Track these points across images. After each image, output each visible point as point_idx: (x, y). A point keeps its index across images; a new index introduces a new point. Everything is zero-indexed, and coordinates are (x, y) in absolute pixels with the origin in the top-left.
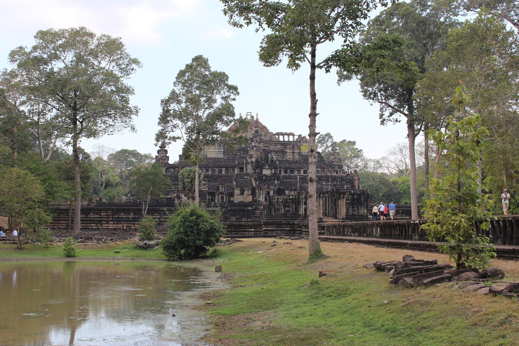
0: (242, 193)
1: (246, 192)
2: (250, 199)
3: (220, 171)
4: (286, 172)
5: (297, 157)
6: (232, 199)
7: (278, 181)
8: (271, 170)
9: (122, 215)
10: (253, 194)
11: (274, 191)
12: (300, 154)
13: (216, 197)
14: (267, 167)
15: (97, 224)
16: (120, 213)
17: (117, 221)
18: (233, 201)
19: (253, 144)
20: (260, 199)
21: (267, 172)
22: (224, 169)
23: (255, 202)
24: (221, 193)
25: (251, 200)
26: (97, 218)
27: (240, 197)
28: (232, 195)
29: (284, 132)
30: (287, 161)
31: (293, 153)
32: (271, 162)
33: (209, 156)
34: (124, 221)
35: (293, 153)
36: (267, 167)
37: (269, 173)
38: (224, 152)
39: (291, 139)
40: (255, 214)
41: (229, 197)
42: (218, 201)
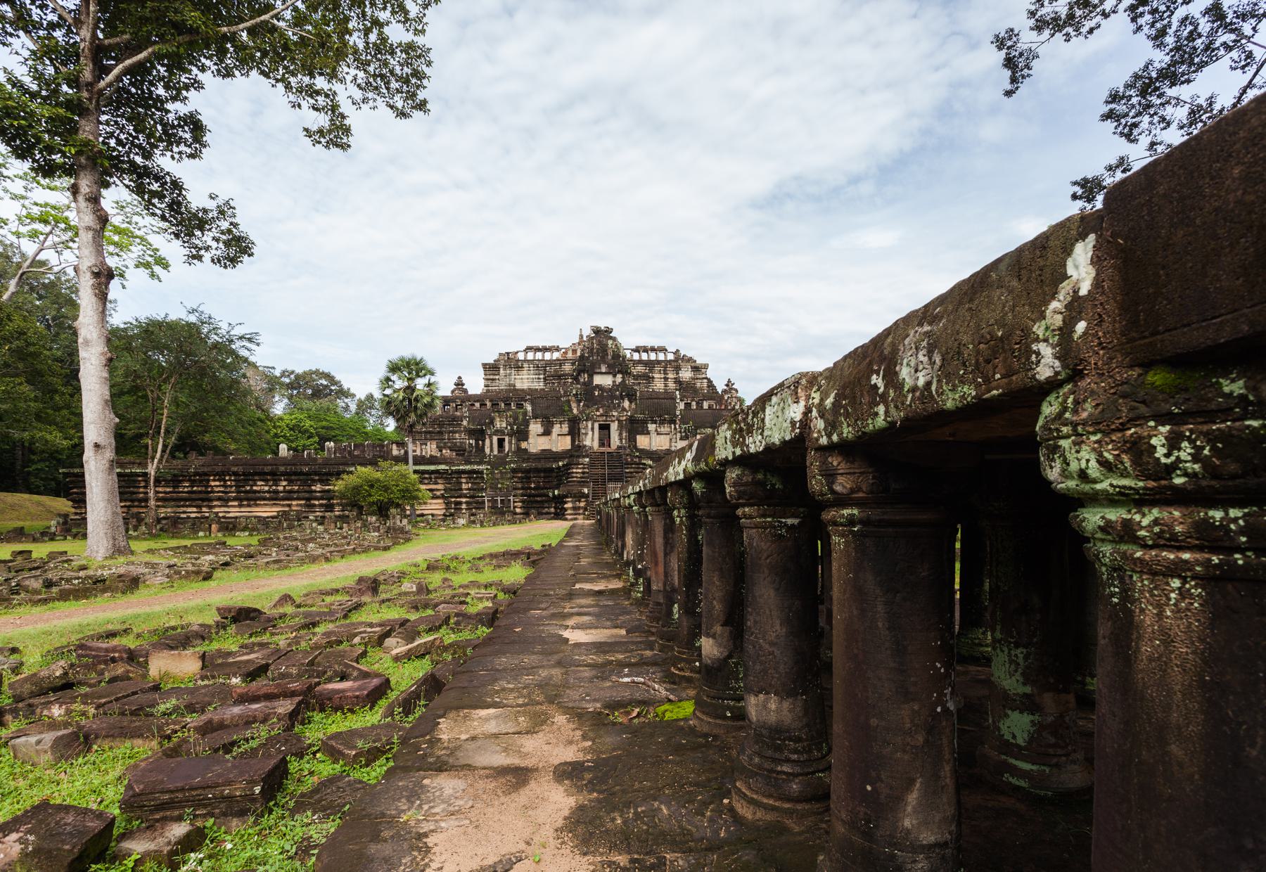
0: (547, 433)
1: (556, 429)
2: (565, 444)
5: (672, 385)
6: (524, 445)
8: (615, 376)
9: (260, 486)
10: (574, 432)
13: (487, 442)
15: (199, 507)
16: (255, 481)
17: (248, 499)
20: (588, 442)
23: (577, 450)
24: (497, 432)
26: (200, 492)
27: (543, 439)
28: (523, 435)
31: (666, 379)
33: (519, 386)
34: (265, 499)
35: (666, 379)
39: (661, 357)
40: (569, 475)
42: (492, 450)
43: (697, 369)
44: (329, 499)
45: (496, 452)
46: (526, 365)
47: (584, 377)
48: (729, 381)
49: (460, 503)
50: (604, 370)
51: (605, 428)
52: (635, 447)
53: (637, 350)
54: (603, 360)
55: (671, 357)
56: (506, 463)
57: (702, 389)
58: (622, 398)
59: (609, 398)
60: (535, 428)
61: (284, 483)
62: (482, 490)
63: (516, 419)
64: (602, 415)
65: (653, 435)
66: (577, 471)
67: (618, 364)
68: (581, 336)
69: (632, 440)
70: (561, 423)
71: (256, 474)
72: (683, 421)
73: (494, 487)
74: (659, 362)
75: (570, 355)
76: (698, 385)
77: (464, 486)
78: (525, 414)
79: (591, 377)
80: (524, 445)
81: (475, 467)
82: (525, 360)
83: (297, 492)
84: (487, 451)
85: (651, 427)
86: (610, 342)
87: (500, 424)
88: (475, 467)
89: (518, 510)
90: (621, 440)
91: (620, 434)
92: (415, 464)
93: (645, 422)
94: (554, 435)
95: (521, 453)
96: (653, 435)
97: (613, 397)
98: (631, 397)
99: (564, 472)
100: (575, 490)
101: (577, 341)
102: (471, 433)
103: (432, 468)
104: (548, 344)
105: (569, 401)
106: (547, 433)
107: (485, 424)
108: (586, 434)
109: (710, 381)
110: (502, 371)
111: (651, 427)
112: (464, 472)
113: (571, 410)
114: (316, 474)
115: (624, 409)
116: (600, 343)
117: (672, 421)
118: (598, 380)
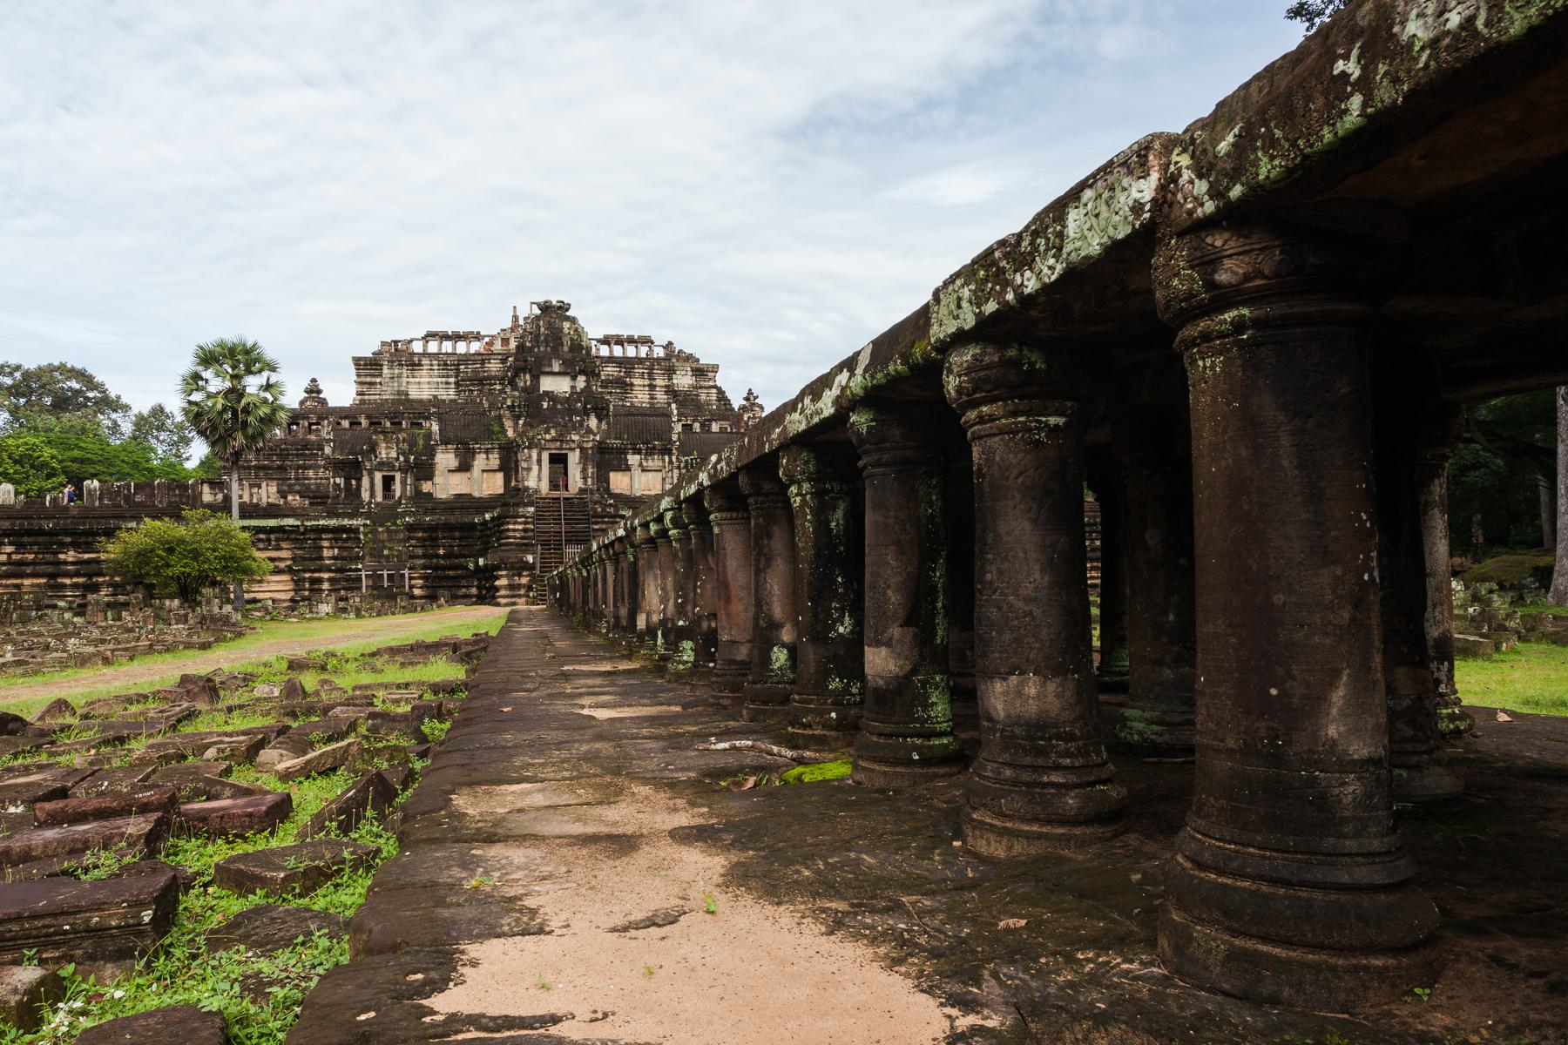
0: (465, 467)
1: (480, 461)
2: (494, 485)
5: (661, 397)
6: (426, 487)
8: (574, 378)
10: (509, 467)
11: (582, 449)
13: (365, 481)
14: (556, 367)
18: (429, 494)
20: (531, 483)
21: (556, 385)
23: (514, 496)
24: (382, 465)
25: (501, 491)
28: (424, 470)
29: (625, 333)
32: (571, 350)
33: (414, 394)
35: (652, 387)
36: (556, 367)
37: (567, 389)
38: (457, 383)
40: (502, 534)
41: (418, 479)
42: (372, 495)
43: (700, 372)
44: (90, 576)
45: (379, 498)
46: (425, 361)
47: (525, 380)
48: (750, 392)
49: (320, 581)
50: (556, 368)
51: (559, 460)
52: (607, 490)
53: (606, 341)
54: (556, 353)
55: (659, 352)
56: (398, 516)
57: (708, 403)
58: (586, 413)
59: (565, 412)
60: (445, 459)
61: (9, 549)
62: (357, 558)
64: (553, 440)
65: (636, 472)
66: (515, 528)
67: (579, 359)
68: (515, 318)
69: (602, 479)
70: (487, 452)
72: (683, 451)
73: (376, 555)
74: (640, 361)
75: (498, 347)
76: (703, 397)
77: (326, 553)
78: (429, 436)
79: (536, 379)
80: (426, 487)
81: (346, 522)
82: (425, 354)
83: (33, 563)
84: (365, 496)
85: (633, 459)
86: (566, 325)
87: (386, 452)
88: (346, 522)
89: (417, 592)
90: (585, 478)
91: (584, 470)
92: (242, 517)
93: (622, 452)
94: (476, 470)
95: (423, 501)
96: (636, 472)
97: (571, 411)
98: (601, 411)
99: (494, 530)
100: (513, 557)
102: (338, 466)
103: (272, 523)
104: (462, 329)
105: (500, 418)
106: (465, 467)
107: (362, 452)
108: (529, 469)
109: (720, 392)
110: (386, 371)
111: (633, 459)
112: (326, 529)
113: (504, 431)
114: (66, 533)
115: (589, 431)
116: (550, 326)
117: (666, 451)
118: (548, 384)
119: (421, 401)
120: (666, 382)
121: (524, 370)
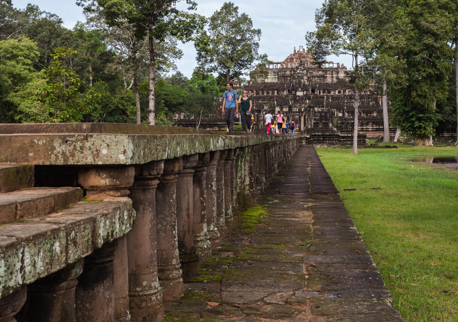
3: (273, 93)
4: (324, 92)
5: (335, 80)
7: (309, 100)
12: (337, 78)
19: (298, 71)
21: (300, 94)
22: (276, 91)
30: (327, 83)
31: (332, 77)
32: (303, 85)
35: (332, 77)
38: (278, 78)
54: (300, 87)
55: (335, 66)
58: (306, 99)
63: (271, 106)
68: (295, 50)
71: (189, 125)
78: (274, 104)
98: (309, 99)
101: (293, 53)
104: (279, 61)
105: (288, 100)
114: (208, 125)
115: (306, 104)
119: (268, 83)
120: (337, 76)
121: (293, 90)
